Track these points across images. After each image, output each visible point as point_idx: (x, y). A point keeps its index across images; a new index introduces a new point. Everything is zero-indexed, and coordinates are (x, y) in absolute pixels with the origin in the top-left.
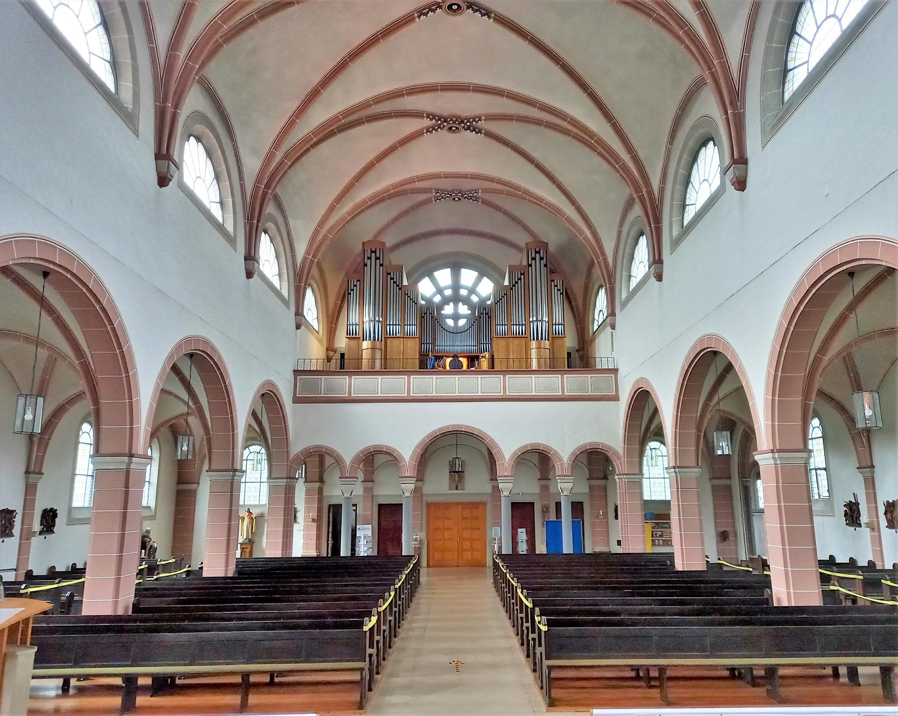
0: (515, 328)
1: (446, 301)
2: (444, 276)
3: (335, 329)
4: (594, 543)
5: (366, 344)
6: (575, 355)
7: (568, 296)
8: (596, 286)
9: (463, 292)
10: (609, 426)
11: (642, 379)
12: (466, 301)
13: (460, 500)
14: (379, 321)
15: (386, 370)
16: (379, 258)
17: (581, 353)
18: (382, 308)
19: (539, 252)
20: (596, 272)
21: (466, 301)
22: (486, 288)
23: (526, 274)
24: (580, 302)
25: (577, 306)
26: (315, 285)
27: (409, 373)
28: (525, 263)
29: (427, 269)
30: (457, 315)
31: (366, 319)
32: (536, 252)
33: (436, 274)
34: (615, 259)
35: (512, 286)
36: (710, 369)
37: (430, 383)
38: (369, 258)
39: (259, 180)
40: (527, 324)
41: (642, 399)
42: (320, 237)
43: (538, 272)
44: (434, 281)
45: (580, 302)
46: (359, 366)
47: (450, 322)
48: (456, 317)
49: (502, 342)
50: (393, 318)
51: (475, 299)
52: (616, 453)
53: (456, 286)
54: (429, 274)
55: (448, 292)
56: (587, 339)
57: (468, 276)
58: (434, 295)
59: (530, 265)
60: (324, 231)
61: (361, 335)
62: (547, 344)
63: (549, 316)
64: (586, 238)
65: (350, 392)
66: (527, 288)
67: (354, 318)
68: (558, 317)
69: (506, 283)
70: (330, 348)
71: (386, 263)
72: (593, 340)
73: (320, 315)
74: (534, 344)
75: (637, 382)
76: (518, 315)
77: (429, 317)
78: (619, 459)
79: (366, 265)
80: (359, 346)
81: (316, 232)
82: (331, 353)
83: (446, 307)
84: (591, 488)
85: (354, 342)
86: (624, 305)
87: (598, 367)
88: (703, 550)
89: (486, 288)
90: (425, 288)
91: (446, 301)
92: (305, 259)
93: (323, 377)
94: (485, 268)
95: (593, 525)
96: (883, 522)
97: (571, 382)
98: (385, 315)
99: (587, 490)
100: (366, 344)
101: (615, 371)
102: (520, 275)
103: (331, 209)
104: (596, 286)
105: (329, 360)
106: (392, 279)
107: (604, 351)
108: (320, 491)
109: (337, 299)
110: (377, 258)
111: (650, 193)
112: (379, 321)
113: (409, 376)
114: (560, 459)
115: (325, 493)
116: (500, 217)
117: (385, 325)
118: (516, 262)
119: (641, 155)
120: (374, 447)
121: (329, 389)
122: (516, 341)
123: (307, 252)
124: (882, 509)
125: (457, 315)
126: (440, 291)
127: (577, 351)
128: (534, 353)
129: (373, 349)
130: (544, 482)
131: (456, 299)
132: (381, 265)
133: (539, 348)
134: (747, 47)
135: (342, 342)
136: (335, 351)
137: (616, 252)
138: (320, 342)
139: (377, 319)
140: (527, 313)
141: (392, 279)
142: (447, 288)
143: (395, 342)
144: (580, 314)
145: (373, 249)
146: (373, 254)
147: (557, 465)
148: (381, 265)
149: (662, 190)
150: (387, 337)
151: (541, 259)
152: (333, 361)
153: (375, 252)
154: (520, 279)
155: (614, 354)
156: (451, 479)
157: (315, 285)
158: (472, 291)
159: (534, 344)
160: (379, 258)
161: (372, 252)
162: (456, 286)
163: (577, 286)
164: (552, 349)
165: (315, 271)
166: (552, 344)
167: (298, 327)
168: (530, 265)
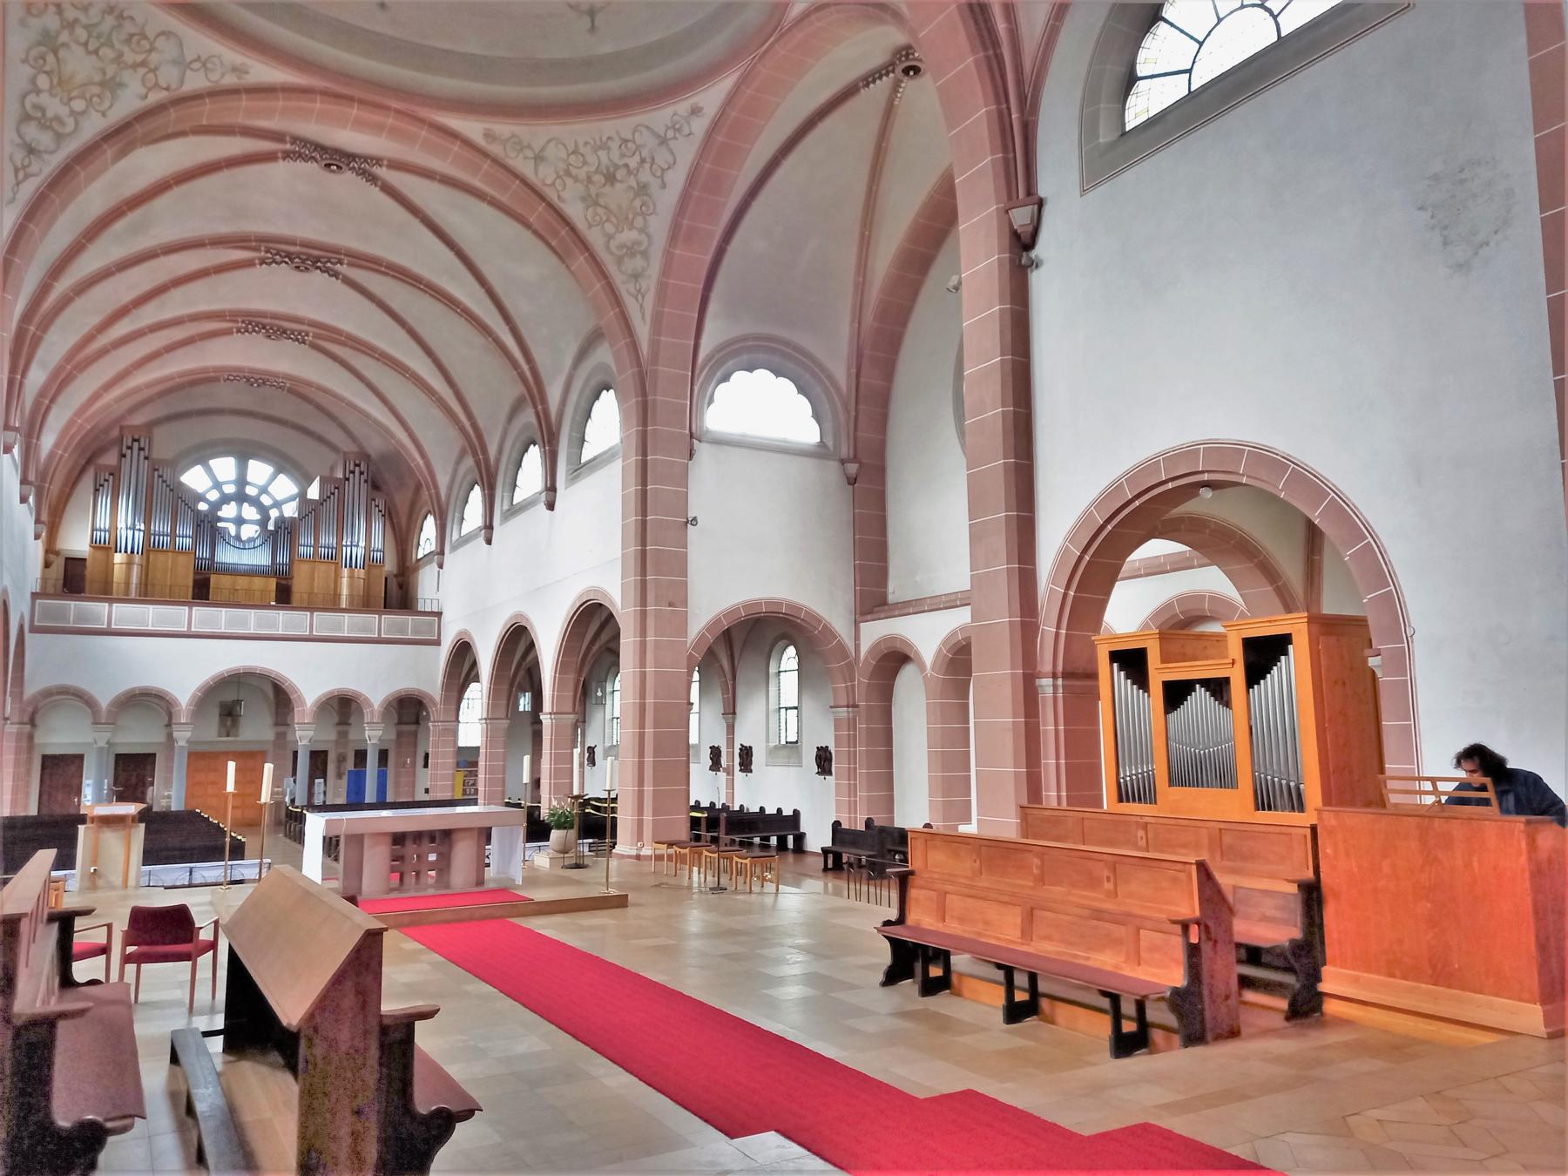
2: (225, 467)
4: (397, 794)
7: (390, 515)
8: (424, 511)
10: (425, 671)
11: (465, 632)
12: (255, 502)
13: (232, 748)
15: (148, 593)
18: (146, 511)
20: (425, 494)
21: (255, 502)
22: (284, 487)
24: (404, 519)
28: (340, 475)
29: (201, 454)
31: (121, 524)
33: (212, 462)
34: (449, 496)
36: (517, 639)
38: (130, 448)
39: (42, 394)
41: (463, 650)
42: (74, 430)
43: (357, 490)
44: (209, 471)
45: (404, 519)
47: (232, 529)
48: (240, 521)
50: (160, 526)
52: (432, 699)
53: (242, 481)
54: (203, 461)
55: (230, 489)
57: (259, 471)
62: (361, 573)
63: (366, 540)
65: (109, 623)
66: (341, 502)
67: (103, 521)
68: (377, 542)
72: (416, 569)
74: (345, 572)
75: (461, 633)
77: (208, 528)
78: (435, 704)
81: (71, 423)
82: (52, 557)
84: (400, 735)
85: (100, 554)
86: (454, 548)
87: (420, 608)
88: (503, 792)
90: (194, 479)
91: (225, 499)
92: (52, 455)
94: (283, 462)
95: (397, 775)
96: (737, 768)
98: (147, 522)
99: (393, 736)
101: (439, 614)
102: (333, 488)
103: (95, 397)
104: (424, 511)
105: (47, 565)
107: (427, 587)
108: (31, 737)
109: (65, 485)
110: (141, 449)
111: (487, 460)
114: (370, 705)
115: (38, 740)
117: (147, 533)
119: (481, 423)
120: (140, 689)
121: (81, 617)
122: (323, 567)
123: (57, 445)
124: (737, 752)
126: (217, 485)
128: (345, 581)
129: (129, 564)
130: (341, 728)
131: (241, 498)
133: (351, 577)
134: (563, 402)
136: (57, 553)
137: (450, 488)
143: (161, 557)
144: (403, 538)
147: (366, 711)
149: (498, 461)
150: (150, 548)
152: (54, 567)
155: (440, 595)
156: (222, 723)
158: (264, 490)
159: (345, 572)
162: (242, 481)
163: (402, 501)
164: (367, 580)
166: (368, 574)
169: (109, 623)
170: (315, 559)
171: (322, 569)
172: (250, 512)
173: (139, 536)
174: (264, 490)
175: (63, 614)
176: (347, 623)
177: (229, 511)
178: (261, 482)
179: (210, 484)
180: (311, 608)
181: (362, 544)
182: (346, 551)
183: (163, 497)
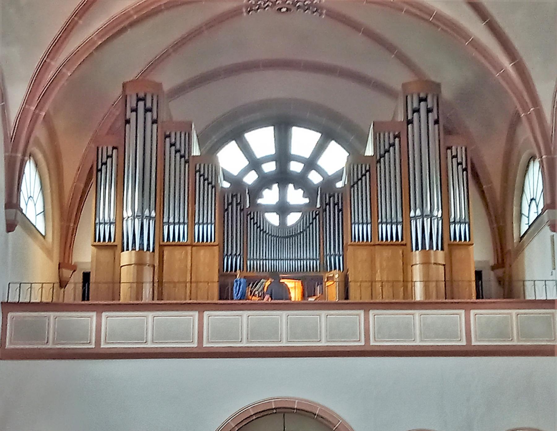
0: (384, 229)
1: (265, 182)
2: (262, 140)
3: (75, 229)
5: (126, 257)
6: (489, 277)
9: (296, 167)
12: (300, 181)
14: (150, 218)
16: (150, 110)
17: (500, 272)
19: (425, 100)
20: (524, 133)
22: (335, 159)
23: (403, 138)
25: (491, 189)
26: (40, 156)
27: (201, 307)
28: (401, 118)
30: (283, 206)
31: (128, 213)
32: (421, 100)
35: (379, 158)
37: (241, 324)
38: (135, 110)
40: (406, 222)
42: (50, 75)
43: (423, 134)
45: (497, 182)
46: (115, 293)
47: (273, 219)
48: (283, 209)
49: (363, 254)
51: (315, 178)
53: (283, 155)
54: (237, 135)
55: (270, 167)
56: (509, 247)
57: (303, 140)
58: (245, 171)
59: (410, 122)
60: (56, 64)
61: (118, 242)
62: (440, 257)
64: (505, 76)
65: (98, 342)
67: (107, 212)
69: (369, 151)
70: (65, 263)
71: (163, 117)
72: (520, 249)
73: (49, 207)
74: (417, 257)
76: (389, 207)
79: (128, 122)
80: (116, 260)
81: (43, 66)
82: (67, 273)
83: (266, 192)
85: (106, 255)
87: (530, 296)
89: (335, 159)
91: (265, 182)
92: (23, 112)
93: (52, 314)
97: (485, 321)
100: (126, 257)
102: (393, 138)
103: (69, 28)
105: (63, 284)
106: (172, 145)
110: (147, 110)
112: (150, 218)
113: (201, 313)
116: (359, 39)
117: (160, 223)
118: (387, 117)
122: (386, 253)
123: (27, 101)
125: (283, 206)
126: (255, 164)
127: (493, 268)
129: (140, 264)
131: (283, 178)
132: (154, 122)
133: (426, 263)
135: (85, 255)
138: (49, 252)
139: (147, 213)
140: (406, 207)
141: (172, 145)
142: (267, 159)
143: (178, 253)
145: (141, 95)
146: (141, 104)
148: (154, 122)
151: (429, 111)
153: (144, 99)
154: (393, 145)
157: (40, 156)
158: (311, 164)
159: (417, 257)
160: (150, 110)
161: (139, 100)
162: (283, 155)
165: (40, 132)
166: (449, 257)
167: (10, 227)
168: (410, 122)
169: (98, 342)
170: (375, 244)
171: (384, 255)
172: (296, 196)
173: (149, 227)
174: (311, 164)
175: (38, 332)
176: (418, 325)
177: (270, 196)
178: (307, 154)
179: (245, 162)
180: (366, 306)
181: (438, 213)
182: (416, 226)
183: (177, 174)
